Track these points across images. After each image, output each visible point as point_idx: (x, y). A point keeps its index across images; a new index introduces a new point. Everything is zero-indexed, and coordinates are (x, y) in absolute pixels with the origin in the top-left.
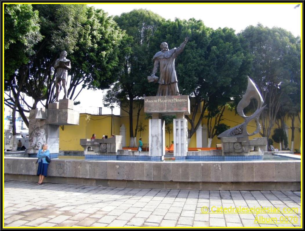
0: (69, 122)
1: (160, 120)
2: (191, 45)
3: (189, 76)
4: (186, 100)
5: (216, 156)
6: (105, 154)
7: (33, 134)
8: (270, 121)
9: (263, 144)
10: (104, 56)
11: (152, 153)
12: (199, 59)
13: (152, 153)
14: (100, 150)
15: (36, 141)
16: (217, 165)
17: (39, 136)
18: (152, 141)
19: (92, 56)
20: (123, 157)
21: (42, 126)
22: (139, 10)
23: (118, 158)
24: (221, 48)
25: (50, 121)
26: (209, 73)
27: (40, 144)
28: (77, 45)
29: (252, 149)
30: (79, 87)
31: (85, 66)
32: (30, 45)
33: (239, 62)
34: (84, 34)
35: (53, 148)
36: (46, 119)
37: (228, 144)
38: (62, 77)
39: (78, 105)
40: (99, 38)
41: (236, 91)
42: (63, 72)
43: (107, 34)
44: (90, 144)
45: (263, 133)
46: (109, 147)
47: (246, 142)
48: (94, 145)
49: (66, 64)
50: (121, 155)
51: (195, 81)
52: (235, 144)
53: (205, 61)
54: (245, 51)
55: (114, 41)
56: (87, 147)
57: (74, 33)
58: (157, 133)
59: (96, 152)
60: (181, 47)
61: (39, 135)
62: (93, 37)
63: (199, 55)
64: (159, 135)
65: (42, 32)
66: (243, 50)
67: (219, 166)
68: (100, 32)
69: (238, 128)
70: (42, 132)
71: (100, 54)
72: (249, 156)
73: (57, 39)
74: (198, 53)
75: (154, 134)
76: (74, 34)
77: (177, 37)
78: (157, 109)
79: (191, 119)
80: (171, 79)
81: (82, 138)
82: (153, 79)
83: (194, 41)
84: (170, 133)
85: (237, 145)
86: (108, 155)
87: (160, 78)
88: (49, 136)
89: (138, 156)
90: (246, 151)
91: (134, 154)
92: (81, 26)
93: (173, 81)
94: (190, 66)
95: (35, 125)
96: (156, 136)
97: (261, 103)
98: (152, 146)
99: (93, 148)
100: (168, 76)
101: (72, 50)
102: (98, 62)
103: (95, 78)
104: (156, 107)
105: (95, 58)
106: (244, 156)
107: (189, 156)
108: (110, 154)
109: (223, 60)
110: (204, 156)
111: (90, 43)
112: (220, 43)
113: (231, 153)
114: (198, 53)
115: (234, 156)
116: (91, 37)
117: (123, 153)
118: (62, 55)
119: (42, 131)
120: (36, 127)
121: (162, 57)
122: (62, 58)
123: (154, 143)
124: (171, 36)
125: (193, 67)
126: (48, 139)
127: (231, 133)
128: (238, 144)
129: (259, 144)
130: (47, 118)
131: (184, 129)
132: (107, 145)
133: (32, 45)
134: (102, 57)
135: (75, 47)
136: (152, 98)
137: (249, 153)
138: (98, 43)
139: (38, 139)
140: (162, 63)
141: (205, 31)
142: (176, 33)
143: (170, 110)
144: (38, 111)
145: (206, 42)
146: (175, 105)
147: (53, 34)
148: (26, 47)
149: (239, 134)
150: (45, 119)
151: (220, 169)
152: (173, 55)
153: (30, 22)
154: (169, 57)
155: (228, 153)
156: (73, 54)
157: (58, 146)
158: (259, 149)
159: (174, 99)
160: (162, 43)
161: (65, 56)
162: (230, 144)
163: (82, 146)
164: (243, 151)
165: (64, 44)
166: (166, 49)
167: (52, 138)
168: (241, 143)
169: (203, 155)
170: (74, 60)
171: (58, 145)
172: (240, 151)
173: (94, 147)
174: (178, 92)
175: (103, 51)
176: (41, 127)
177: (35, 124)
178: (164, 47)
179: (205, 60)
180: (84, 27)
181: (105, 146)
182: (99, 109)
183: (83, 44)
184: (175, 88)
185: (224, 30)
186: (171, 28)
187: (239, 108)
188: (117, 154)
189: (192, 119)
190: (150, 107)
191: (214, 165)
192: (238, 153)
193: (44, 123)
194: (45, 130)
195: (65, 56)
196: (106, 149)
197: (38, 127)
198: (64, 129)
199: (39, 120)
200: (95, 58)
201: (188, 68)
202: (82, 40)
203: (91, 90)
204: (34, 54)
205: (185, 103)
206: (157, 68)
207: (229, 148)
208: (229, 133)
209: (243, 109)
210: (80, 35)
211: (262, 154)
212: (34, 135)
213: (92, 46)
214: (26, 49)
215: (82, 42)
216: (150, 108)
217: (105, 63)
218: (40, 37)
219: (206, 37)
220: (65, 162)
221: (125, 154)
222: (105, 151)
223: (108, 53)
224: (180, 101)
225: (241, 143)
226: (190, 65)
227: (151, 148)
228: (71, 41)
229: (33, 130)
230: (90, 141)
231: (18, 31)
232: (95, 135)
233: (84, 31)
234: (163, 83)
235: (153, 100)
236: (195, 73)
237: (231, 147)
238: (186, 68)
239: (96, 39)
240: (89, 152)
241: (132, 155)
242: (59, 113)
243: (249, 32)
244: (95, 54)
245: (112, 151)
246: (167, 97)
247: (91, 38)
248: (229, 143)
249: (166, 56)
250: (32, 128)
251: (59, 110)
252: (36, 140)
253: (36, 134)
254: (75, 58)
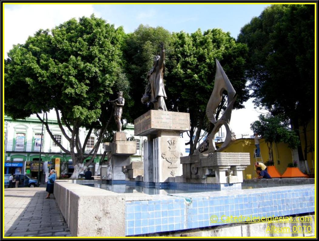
19: (188, 83)
35: (121, 175)
37: (186, 165)
38: (115, 115)
47: (198, 162)
52: (193, 166)
88: (114, 165)
126: (114, 167)
207: (187, 173)
223: (203, 74)
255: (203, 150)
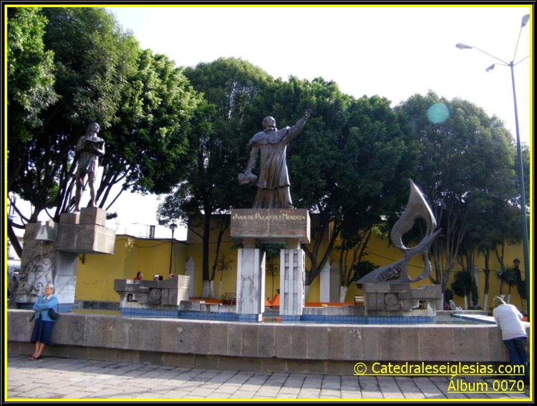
0: (96, 248)
1: (257, 251)
2: (315, 124)
3: (311, 177)
4: (304, 217)
5: (354, 316)
6: (158, 308)
7: (30, 268)
8: (447, 259)
9: (434, 297)
10: (164, 136)
11: (241, 309)
12: (328, 147)
13: (241, 309)
14: (150, 299)
15: (33, 280)
16: (355, 330)
17: (40, 271)
18: (243, 287)
19: (142, 135)
20: (189, 314)
21: (47, 254)
22: (228, 60)
23: (180, 315)
24: (367, 131)
25: (61, 245)
26: (345, 173)
27: (41, 285)
28: (118, 114)
29: (417, 305)
30: (116, 188)
31: (130, 151)
32: (34, 110)
33: (397, 156)
34: (131, 96)
35: (65, 294)
36: (54, 240)
37: (374, 295)
38: (88, 168)
39: (113, 219)
40: (156, 104)
41: (391, 205)
42: (91, 161)
43: (171, 97)
44: (131, 289)
45: (435, 280)
46: (166, 295)
47: (405, 293)
48: (138, 292)
49: (97, 146)
50: (186, 310)
51: (321, 186)
52: (387, 296)
53: (339, 151)
54: (406, 137)
55: (183, 111)
56: (127, 295)
57: (113, 93)
58: (251, 274)
59: (141, 304)
60: (299, 125)
61: (39, 269)
62: (147, 101)
63: (328, 141)
64: (255, 277)
65: (57, 88)
66: (403, 136)
67: (359, 333)
68: (159, 94)
69: (392, 269)
70: (47, 265)
71: (157, 132)
72: (411, 317)
73: (83, 103)
74: (327, 137)
75: (246, 275)
76: (114, 94)
77: (291, 108)
78: (253, 231)
79: (311, 252)
80: (279, 178)
81: (117, 278)
82: (247, 178)
83: (321, 117)
84: (273, 276)
85: (391, 298)
86: (164, 310)
87: (260, 178)
88: (58, 272)
89: (216, 313)
90: (406, 309)
91: (209, 310)
92: (127, 82)
93: (281, 184)
94: (312, 159)
95: (34, 252)
96: (249, 278)
97: (433, 225)
98: (242, 296)
99: (136, 297)
100: (273, 173)
101: (109, 122)
102: (153, 144)
103: (146, 172)
104: (251, 228)
105: (148, 138)
106: (402, 317)
107: (307, 315)
108: (167, 308)
109: (369, 152)
110: (332, 316)
111: (140, 112)
112: (366, 122)
113: (381, 310)
114: (327, 137)
115: (384, 317)
116: (143, 102)
117: (190, 307)
118: (91, 130)
119: (46, 263)
120: (35, 255)
121: (265, 142)
122: (91, 136)
123: (246, 291)
124: (282, 106)
125: (317, 161)
126: (57, 276)
127: (381, 277)
128: (392, 296)
129: (428, 296)
130: (57, 239)
131: (298, 268)
132: (163, 291)
133: (38, 110)
134: (161, 137)
135: (113, 117)
136: (245, 212)
137: (410, 313)
138: (154, 112)
139: (37, 277)
140: (265, 151)
141: (339, 100)
142: (289, 101)
143: (275, 233)
144: (41, 227)
145: (342, 119)
146: (284, 225)
147: (76, 93)
148: (27, 113)
149: (395, 278)
150: (52, 240)
151: (360, 337)
152: (284, 139)
153: (37, 70)
154: (276, 142)
155: (374, 311)
156: (109, 129)
157: (73, 290)
158: (429, 306)
159: (283, 214)
160: (266, 118)
161: (96, 132)
162: (378, 295)
163: (117, 292)
164: (401, 307)
165: (95, 111)
166: (273, 129)
167: (63, 276)
168: (397, 294)
169: (331, 314)
170: (111, 140)
171: (74, 289)
172: (395, 308)
173: (139, 294)
174: (289, 203)
175: (162, 127)
176: (45, 255)
177: (33, 250)
178: (269, 125)
179: (338, 150)
180: (131, 83)
181: (158, 293)
182: (149, 228)
183: (129, 112)
184: (286, 195)
185: (373, 100)
186: (281, 93)
187: (395, 234)
188: (179, 309)
189: (314, 250)
190: (241, 227)
191: (349, 330)
192: (391, 311)
193: (51, 248)
194: (52, 260)
195: (96, 132)
196: (161, 298)
197: (39, 255)
198: (85, 261)
199: (42, 242)
200: (148, 138)
201: (310, 163)
202: (127, 105)
203: (138, 195)
204: (41, 126)
205: (301, 222)
206: (255, 161)
208: (377, 276)
209: (402, 235)
210: (124, 98)
211: (434, 313)
212: (31, 269)
213: (145, 117)
214: (26, 116)
215: (127, 110)
216: (240, 229)
217: (165, 148)
218: (54, 98)
219: (341, 111)
220: (86, 318)
221: (193, 309)
222: (158, 302)
223: (171, 131)
224: (293, 218)
225: (397, 294)
226: (312, 157)
227: (240, 299)
228: (107, 106)
229: (28, 260)
230: (133, 283)
231: (15, 84)
232: (142, 274)
233: (131, 90)
234: (265, 187)
235: (247, 214)
236: (322, 171)
237: (380, 301)
238: (305, 162)
239: (151, 105)
240: (130, 303)
241: (205, 310)
242: (78, 231)
243: (415, 105)
244: (148, 130)
245: (170, 303)
246: (270, 211)
247: (143, 104)
248: (377, 293)
249: (272, 141)
250: (29, 256)
251: (80, 226)
252: (34, 278)
253: (34, 267)
254: (113, 137)
255: (391, 278)
